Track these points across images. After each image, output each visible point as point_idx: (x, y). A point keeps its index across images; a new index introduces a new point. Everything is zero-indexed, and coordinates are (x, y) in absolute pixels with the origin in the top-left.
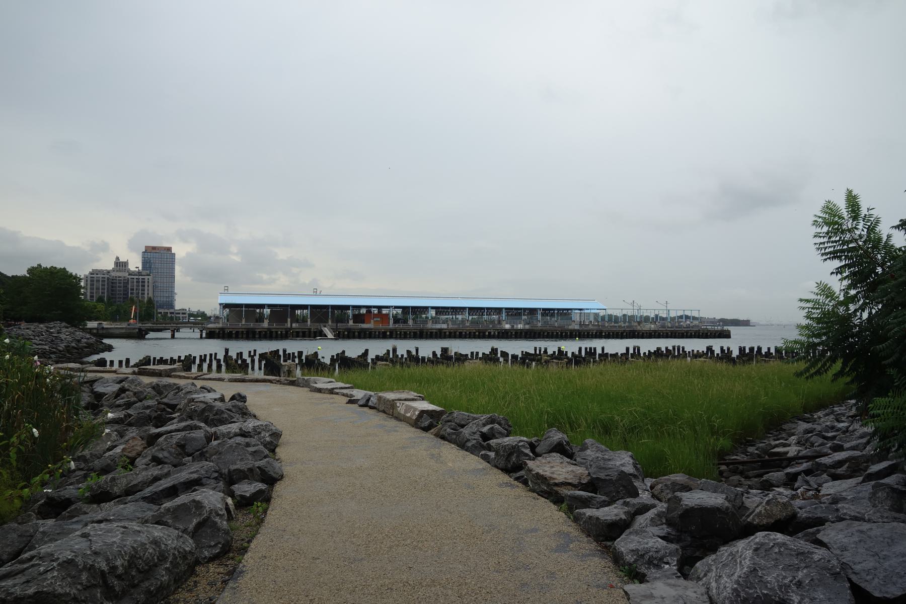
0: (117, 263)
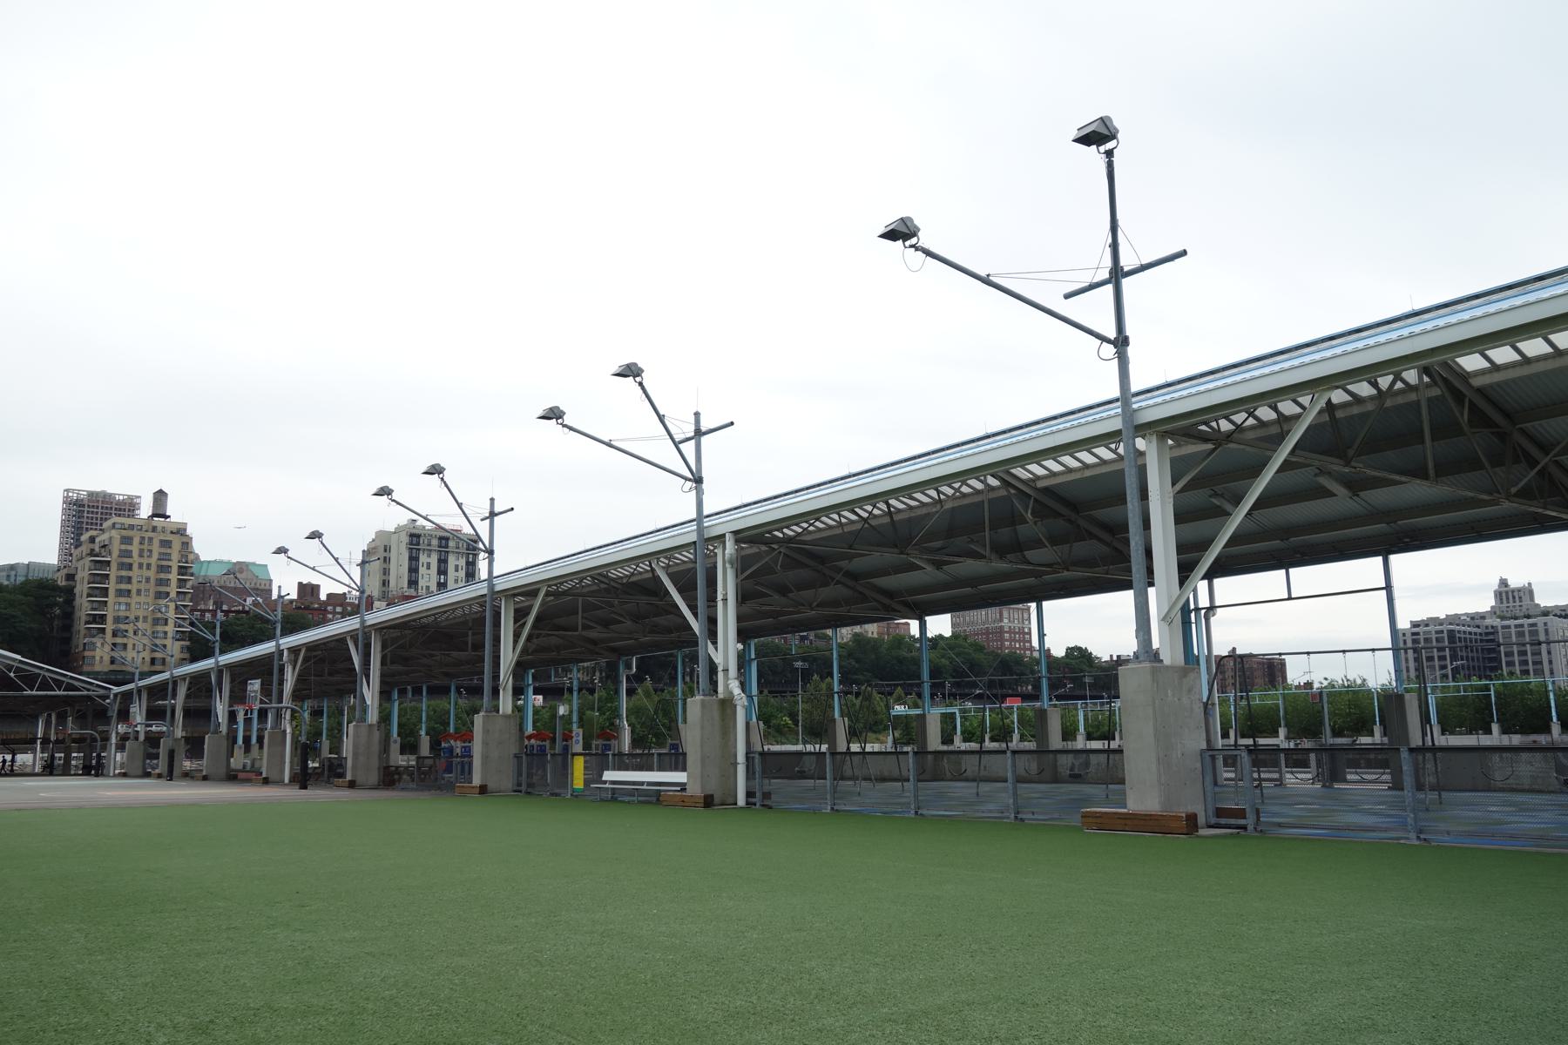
0: (1501, 593)
